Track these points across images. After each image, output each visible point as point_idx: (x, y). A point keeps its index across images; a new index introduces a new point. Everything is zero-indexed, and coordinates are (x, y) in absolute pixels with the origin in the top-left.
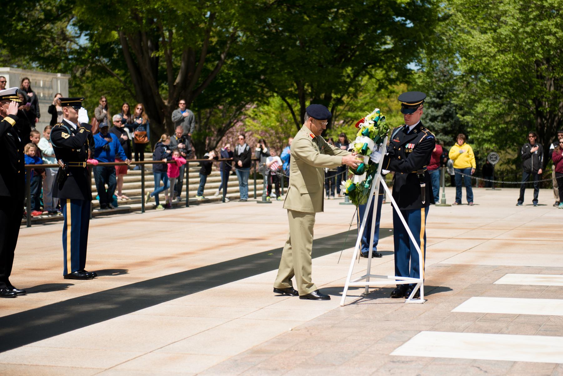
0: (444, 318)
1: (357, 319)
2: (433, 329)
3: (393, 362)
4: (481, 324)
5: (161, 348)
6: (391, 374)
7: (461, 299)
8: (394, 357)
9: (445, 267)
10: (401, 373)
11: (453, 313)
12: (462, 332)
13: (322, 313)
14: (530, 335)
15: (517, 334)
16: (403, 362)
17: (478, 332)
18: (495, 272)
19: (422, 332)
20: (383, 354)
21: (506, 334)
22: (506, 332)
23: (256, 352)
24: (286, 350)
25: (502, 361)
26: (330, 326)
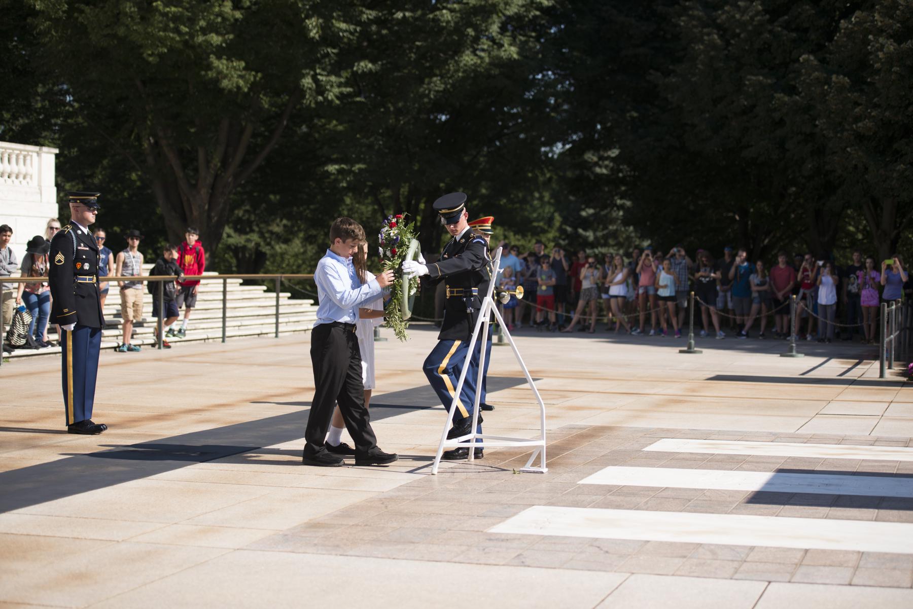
3: (490, 540)
4: (610, 498)
6: (485, 553)
7: (593, 469)
8: (491, 534)
9: (581, 429)
10: (498, 552)
13: (403, 483)
14: (674, 511)
16: (503, 540)
17: (608, 508)
18: (647, 436)
21: (643, 510)
23: (314, 526)
24: (353, 525)
25: (630, 541)
26: (413, 498)
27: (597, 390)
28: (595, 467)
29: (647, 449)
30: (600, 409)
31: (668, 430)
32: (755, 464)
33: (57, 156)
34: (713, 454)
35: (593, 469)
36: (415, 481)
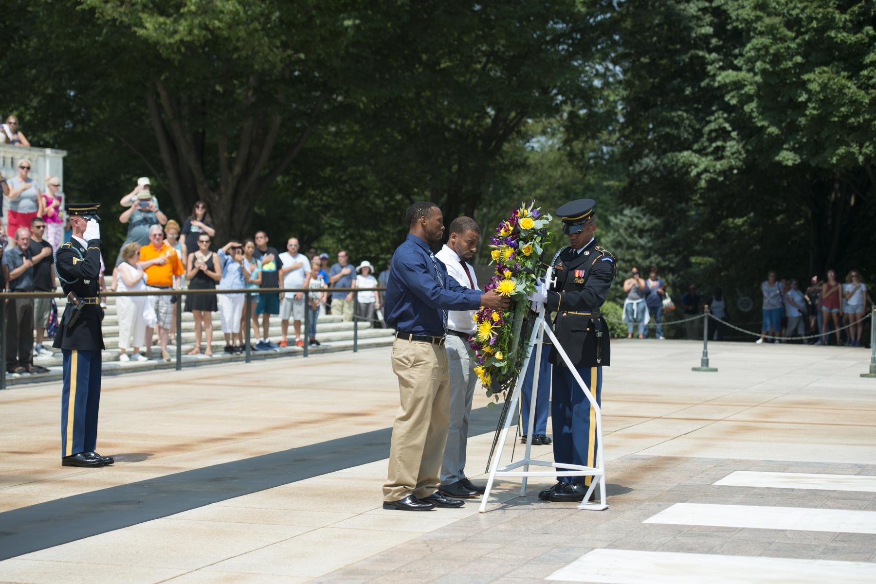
0: (631, 531)
1: (502, 531)
2: (613, 545)
4: (681, 539)
5: (212, 565)
9: (643, 459)
11: (644, 524)
12: (655, 551)
13: (449, 522)
14: (753, 555)
15: (734, 554)
17: (678, 551)
18: (718, 468)
19: (595, 550)
20: (534, 578)
22: (719, 551)
26: (460, 539)
27: (659, 416)
28: (661, 503)
29: (718, 483)
30: (664, 437)
31: (740, 461)
32: (843, 501)
33: (65, 160)
34: (793, 490)
35: (660, 506)
36: (462, 520)
